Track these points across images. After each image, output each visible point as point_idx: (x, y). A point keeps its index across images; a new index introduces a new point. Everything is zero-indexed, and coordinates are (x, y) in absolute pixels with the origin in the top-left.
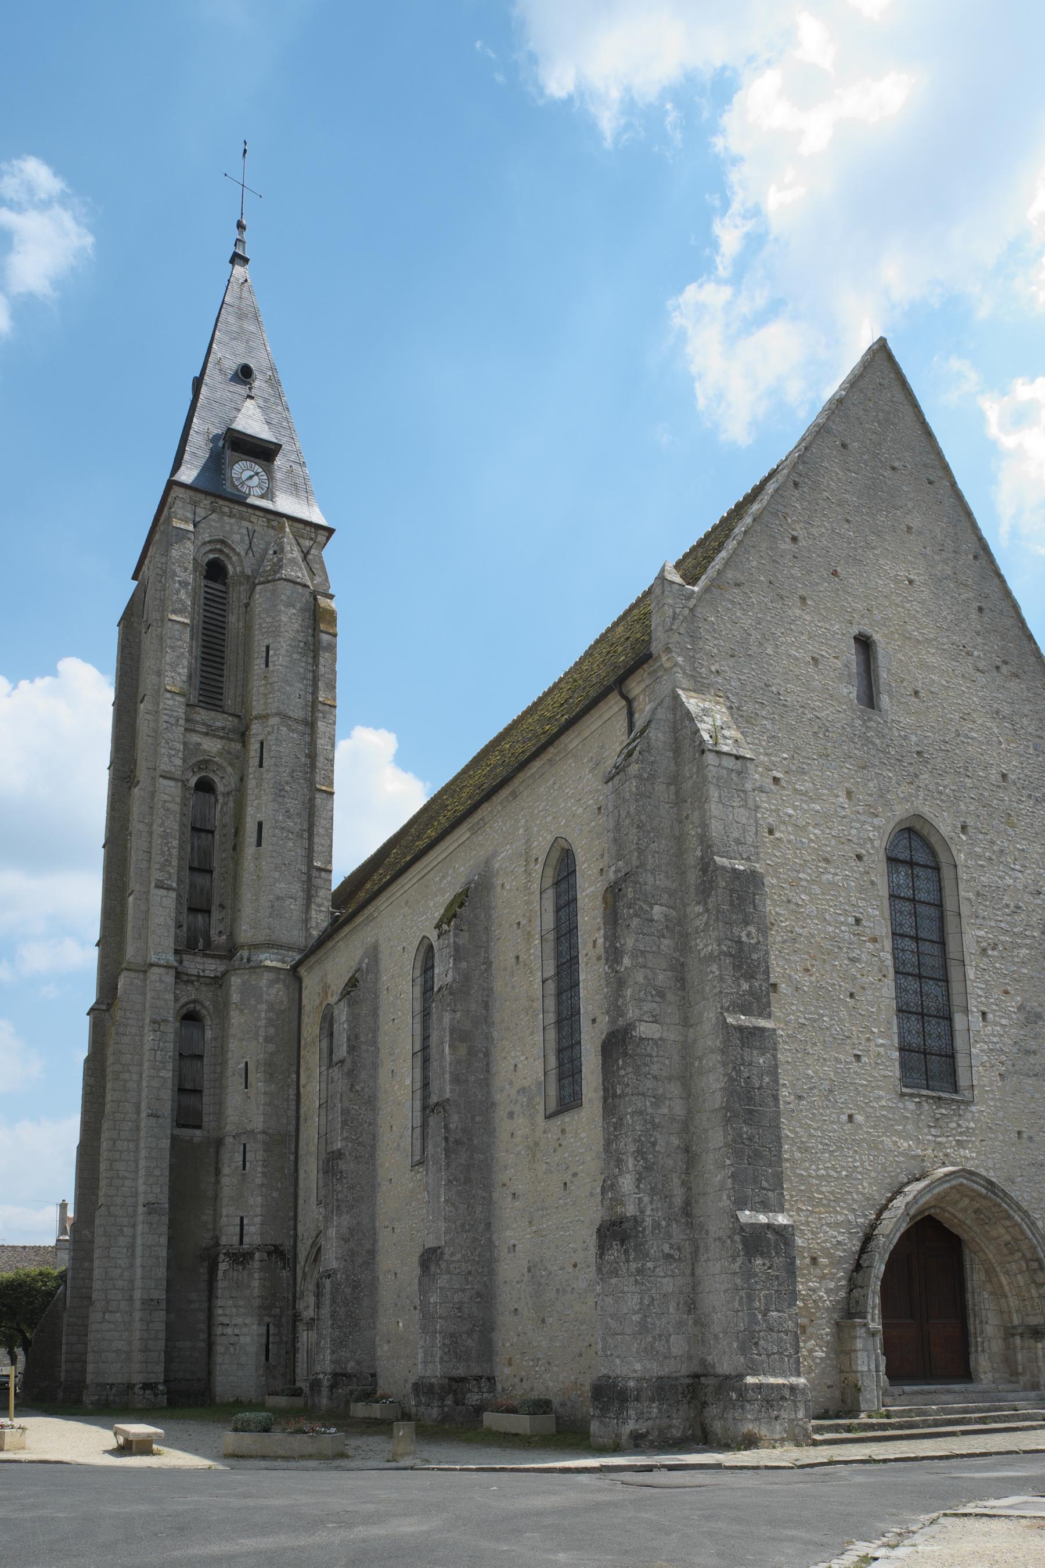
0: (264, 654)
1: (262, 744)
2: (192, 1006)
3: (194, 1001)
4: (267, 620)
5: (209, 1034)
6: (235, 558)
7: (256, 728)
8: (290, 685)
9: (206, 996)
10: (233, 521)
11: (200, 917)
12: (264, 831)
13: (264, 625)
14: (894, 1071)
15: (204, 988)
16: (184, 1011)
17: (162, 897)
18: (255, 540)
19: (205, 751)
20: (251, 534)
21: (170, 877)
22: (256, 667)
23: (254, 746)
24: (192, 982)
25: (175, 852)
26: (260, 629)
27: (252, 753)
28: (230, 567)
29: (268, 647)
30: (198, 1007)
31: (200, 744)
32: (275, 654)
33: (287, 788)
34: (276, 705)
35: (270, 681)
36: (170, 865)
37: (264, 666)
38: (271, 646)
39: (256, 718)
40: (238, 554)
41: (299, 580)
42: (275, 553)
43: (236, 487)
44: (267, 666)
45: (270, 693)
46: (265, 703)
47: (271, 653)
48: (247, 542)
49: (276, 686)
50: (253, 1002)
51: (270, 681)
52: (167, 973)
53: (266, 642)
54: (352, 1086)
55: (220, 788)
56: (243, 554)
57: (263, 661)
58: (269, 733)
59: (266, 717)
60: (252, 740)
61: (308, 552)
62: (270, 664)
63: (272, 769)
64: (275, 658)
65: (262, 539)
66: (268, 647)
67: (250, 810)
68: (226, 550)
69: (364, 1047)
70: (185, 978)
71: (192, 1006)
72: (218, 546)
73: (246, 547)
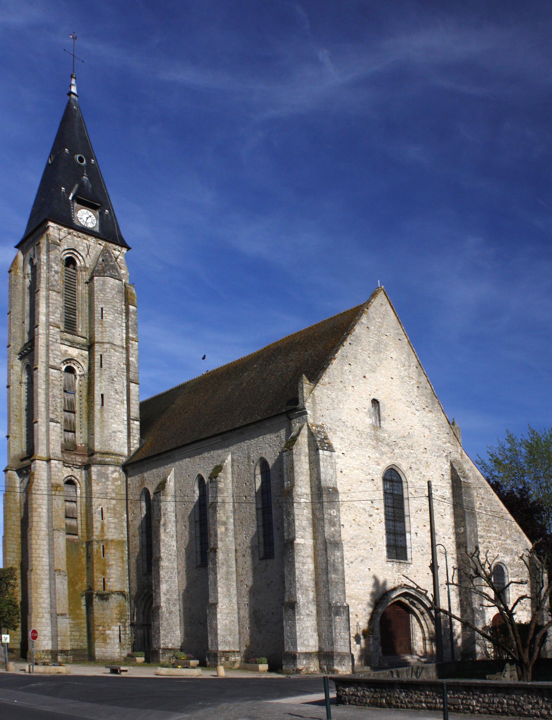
0: (100, 312)
1: (101, 355)
2: (70, 478)
3: (71, 476)
4: (101, 295)
5: (79, 491)
6: (80, 258)
7: (97, 347)
8: (114, 329)
9: (79, 475)
10: (79, 239)
11: (71, 434)
12: (105, 399)
13: (99, 297)
14: (385, 553)
15: (75, 470)
16: (66, 480)
17: (54, 426)
18: (90, 250)
19: (69, 355)
20: (88, 247)
21: (57, 417)
22: (96, 318)
23: (97, 357)
24: (70, 467)
25: (59, 405)
26: (97, 299)
27: (96, 360)
28: (78, 262)
29: (102, 309)
30: (73, 478)
31: (67, 351)
32: (106, 313)
33: (115, 379)
34: (108, 338)
35: (104, 326)
36: (57, 411)
37: (100, 318)
38: (104, 309)
39: (97, 343)
40: (82, 256)
41: (117, 277)
42: (103, 261)
43: (80, 222)
44: (102, 318)
45: (104, 332)
46: (102, 336)
47: (104, 312)
48: (87, 251)
49: (108, 329)
50: (104, 480)
51: (104, 326)
52: (59, 464)
53: (101, 306)
54: (165, 530)
55: (78, 372)
56: (84, 256)
57: (100, 315)
58: (104, 352)
59: (103, 343)
60: (96, 354)
61: (118, 258)
62: (104, 318)
63: (107, 369)
64: (106, 315)
65: (94, 250)
66: (102, 309)
67: (97, 388)
68: (76, 253)
69: (170, 514)
70: (66, 465)
71: (70, 478)
72: (72, 251)
73: (86, 253)
